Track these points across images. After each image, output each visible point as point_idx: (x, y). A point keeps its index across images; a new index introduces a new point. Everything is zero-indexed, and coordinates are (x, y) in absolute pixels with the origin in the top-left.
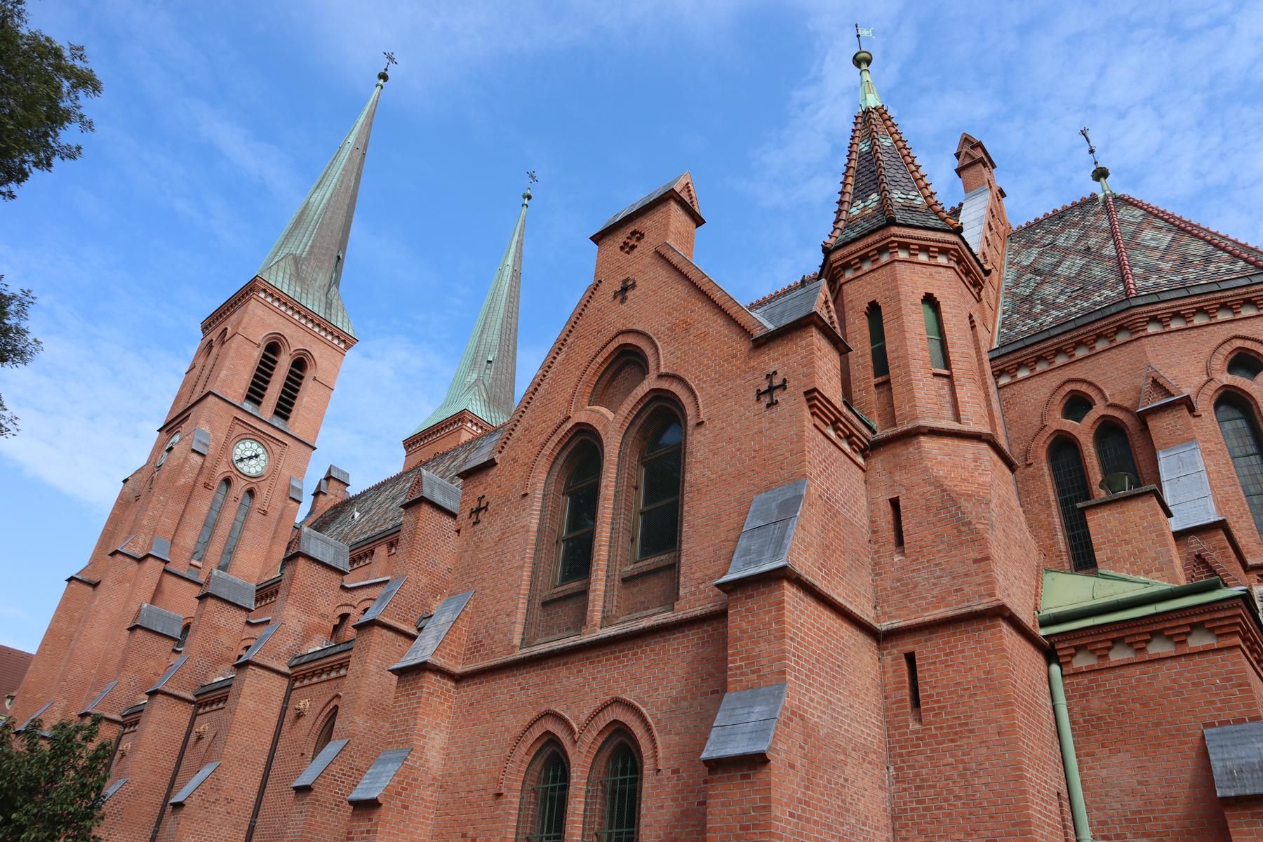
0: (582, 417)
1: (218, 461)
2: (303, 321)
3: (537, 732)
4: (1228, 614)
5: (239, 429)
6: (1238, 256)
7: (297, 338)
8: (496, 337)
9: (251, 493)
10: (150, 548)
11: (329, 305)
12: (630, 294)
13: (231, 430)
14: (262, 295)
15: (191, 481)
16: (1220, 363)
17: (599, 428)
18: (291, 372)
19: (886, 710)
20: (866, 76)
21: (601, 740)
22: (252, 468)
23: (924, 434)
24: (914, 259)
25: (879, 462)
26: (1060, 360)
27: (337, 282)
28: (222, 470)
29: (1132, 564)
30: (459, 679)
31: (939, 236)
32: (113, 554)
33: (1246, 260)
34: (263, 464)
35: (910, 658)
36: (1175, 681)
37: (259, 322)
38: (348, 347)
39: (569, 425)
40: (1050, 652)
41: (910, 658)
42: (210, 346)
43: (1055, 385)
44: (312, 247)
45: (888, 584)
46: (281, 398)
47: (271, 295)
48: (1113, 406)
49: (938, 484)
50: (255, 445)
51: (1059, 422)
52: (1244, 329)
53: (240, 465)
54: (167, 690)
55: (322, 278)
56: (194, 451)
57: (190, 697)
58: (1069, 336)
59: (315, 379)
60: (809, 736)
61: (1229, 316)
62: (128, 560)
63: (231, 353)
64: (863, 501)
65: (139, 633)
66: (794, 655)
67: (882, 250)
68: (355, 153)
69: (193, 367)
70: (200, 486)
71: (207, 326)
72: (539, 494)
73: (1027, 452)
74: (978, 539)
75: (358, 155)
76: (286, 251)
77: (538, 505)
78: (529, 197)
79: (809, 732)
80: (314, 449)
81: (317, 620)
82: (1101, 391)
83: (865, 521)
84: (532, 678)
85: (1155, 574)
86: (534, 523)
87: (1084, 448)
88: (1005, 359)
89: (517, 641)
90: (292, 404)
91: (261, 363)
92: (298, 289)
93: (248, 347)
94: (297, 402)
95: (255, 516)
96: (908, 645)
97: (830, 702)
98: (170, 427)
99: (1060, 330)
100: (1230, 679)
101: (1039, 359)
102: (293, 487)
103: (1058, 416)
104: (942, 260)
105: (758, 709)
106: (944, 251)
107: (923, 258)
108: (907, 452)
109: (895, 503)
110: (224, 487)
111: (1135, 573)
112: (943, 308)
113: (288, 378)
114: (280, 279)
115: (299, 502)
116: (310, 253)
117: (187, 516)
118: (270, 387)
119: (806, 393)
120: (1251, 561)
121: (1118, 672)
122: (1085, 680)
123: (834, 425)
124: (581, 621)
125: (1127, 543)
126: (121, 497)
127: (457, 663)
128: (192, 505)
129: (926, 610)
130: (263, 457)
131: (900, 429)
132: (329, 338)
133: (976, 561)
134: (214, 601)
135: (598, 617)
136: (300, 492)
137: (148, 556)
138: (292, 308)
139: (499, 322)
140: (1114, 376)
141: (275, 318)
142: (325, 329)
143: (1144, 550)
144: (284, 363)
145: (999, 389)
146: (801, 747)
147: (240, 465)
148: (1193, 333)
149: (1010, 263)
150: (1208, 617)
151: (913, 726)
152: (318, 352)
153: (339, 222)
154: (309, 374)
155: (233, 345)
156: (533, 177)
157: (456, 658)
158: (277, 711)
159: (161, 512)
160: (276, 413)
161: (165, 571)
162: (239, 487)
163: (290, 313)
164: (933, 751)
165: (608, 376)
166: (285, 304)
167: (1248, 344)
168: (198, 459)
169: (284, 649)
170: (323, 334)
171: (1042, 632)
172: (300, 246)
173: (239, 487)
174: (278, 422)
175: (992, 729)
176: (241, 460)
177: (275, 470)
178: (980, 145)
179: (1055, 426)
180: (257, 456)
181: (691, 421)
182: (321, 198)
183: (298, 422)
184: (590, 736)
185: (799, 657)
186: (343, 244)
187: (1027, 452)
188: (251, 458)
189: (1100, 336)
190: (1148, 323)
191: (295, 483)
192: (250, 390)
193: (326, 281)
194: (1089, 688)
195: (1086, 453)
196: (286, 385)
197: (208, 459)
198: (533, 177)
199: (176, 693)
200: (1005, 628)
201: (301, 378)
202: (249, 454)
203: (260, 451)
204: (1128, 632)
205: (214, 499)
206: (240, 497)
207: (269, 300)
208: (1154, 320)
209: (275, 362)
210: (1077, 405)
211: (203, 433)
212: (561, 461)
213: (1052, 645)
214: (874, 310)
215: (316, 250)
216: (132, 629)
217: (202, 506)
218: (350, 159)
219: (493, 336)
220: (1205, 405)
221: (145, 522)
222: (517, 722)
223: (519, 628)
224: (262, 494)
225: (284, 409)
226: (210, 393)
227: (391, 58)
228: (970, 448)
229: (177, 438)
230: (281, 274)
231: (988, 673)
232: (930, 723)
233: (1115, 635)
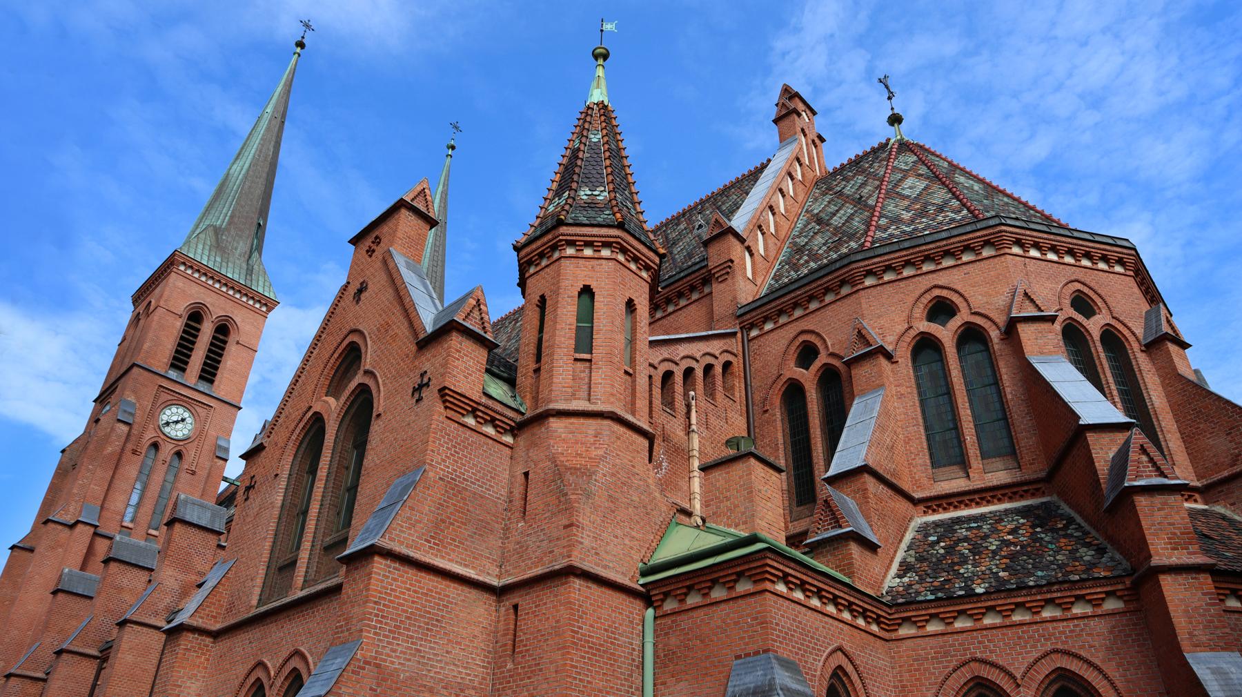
0: (317, 407)
1: (145, 428)
2: (224, 289)
3: (252, 679)
4: (758, 564)
5: (165, 397)
6: (964, 205)
7: (218, 306)
9: (179, 455)
10: (80, 515)
11: (250, 271)
12: (363, 296)
13: (156, 397)
14: (182, 268)
15: (118, 449)
16: (920, 311)
17: (326, 418)
18: (214, 337)
19: (496, 653)
20: (600, 72)
21: (287, 684)
22: (179, 432)
23: (553, 416)
24: (580, 254)
25: (522, 440)
26: (798, 313)
27: (259, 248)
28: (149, 436)
29: (728, 518)
30: (216, 635)
31: (604, 231)
32: (46, 523)
33: (968, 209)
34: (189, 427)
35: (516, 607)
36: (723, 621)
37: (180, 293)
38: (270, 310)
39: (310, 414)
40: (646, 597)
41: (516, 607)
42: (136, 319)
43: (792, 336)
44: (232, 217)
45: (511, 546)
46: (205, 364)
47: (191, 267)
48: (832, 355)
49: (553, 460)
50: (181, 410)
51: (794, 371)
52: (942, 279)
53: (167, 430)
54: (72, 648)
55: (242, 246)
56: (119, 421)
57: (96, 653)
58: (803, 290)
59: (238, 343)
60: (385, 680)
61: (932, 267)
62: (60, 527)
63: (154, 325)
64: (506, 475)
65: (60, 596)
66: (377, 615)
67: (554, 248)
68: (274, 122)
69: (124, 339)
70: (128, 453)
71: (138, 298)
72: (285, 475)
73: (766, 399)
74: (569, 509)
75: (276, 123)
76: (207, 222)
77: (283, 484)
78: (453, 148)
79: (383, 675)
80: (240, 408)
81: (194, 577)
82: (825, 341)
83: (504, 492)
84: (255, 633)
85: (742, 527)
86: (279, 499)
87: (808, 394)
88: (754, 314)
89: (254, 602)
90: (217, 369)
91: (184, 331)
92: (218, 259)
93: (170, 318)
94: (221, 366)
95: (184, 476)
96: (515, 598)
97: (420, 651)
98: (102, 399)
99: (796, 285)
100: (756, 619)
101: (781, 312)
102: (220, 447)
103: (792, 365)
104: (606, 253)
105: (339, 660)
106: (606, 245)
107: (588, 252)
108: (540, 431)
109: (526, 474)
110: (153, 451)
111: (729, 526)
112: (596, 297)
113: (212, 344)
114: (199, 251)
115: (226, 460)
116: (230, 223)
117: (118, 483)
119: (440, 391)
120: (917, 495)
121: (690, 614)
122: (668, 621)
123: (474, 412)
124: (289, 587)
125: (728, 499)
126: (59, 468)
127: (217, 622)
128: (121, 471)
129: (530, 568)
130: (189, 420)
131: (540, 410)
132: (251, 302)
133: (566, 527)
134: (116, 564)
135: (299, 580)
136: (227, 450)
137: (78, 522)
138: (212, 278)
140: (832, 327)
142: (246, 295)
143: (736, 506)
144: (207, 331)
145: (749, 341)
146: (371, 689)
147: (167, 430)
148: (902, 284)
149: (807, 211)
150: (747, 567)
151: (510, 666)
152: (240, 317)
153: (259, 191)
154: (232, 339)
155: (156, 318)
156: (456, 128)
157: (215, 617)
158: (155, 662)
159: (90, 481)
160: (201, 377)
161: (95, 534)
162: (167, 450)
163: (210, 282)
164: (517, 686)
165: (342, 368)
166: (205, 274)
167: (944, 293)
168: (125, 428)
169: (161, 606)
170: (244, 299)
171: (642, 581)
172: (220, 218)
173: (167, 450)
174: (203, 386)
175: (552, 668)
176: (168, 424)
177: (201, 432)
178: (797, 95)
179: (788, 374)
180: (183, 420)
181: (374, 415)
182: (240, 169)
183: (223, 385)
184: (278, 682)
185: (383, 617)
186: (264, 212)
187: (766, 399)
188: (178, 422)
189: (827, 290)
190: (865, 276)
191: (222, 443)
192: (174, 358)
193: (247, 249)
194: (671, 628)
195: (809, 399)
196: (210, 351)
197: (135, 426)
198: (456, 128)
199: (81, 650)
200: (577, 583)
201: (225, 342)
202: (175, 418)
203: (186, 415)
204: (697, 580)
205: (143, 462)
206: (168, 459)
207: (189, 272)
208: (870, 273)
209: (198, 330)
210: (807, 354)
211: (129, 403)
212: (304, 446)
213: (648, 591)
214: (543, 299)
215: (236, 220)
216: (55, 593)
217: (131, 469)
218: (268, 129)
220: (904, 355)
221: (75, 491)
222: (242, 670)
223: (257, 591)
224: (190, 455)
225: (209, 373)
226: (134, 365)
227: (307, 26)
228: (592, 425)
229: (108, 408)
230: (200, 246)
231: (558, 621)
232: (519, 663)
233: (688, 583)
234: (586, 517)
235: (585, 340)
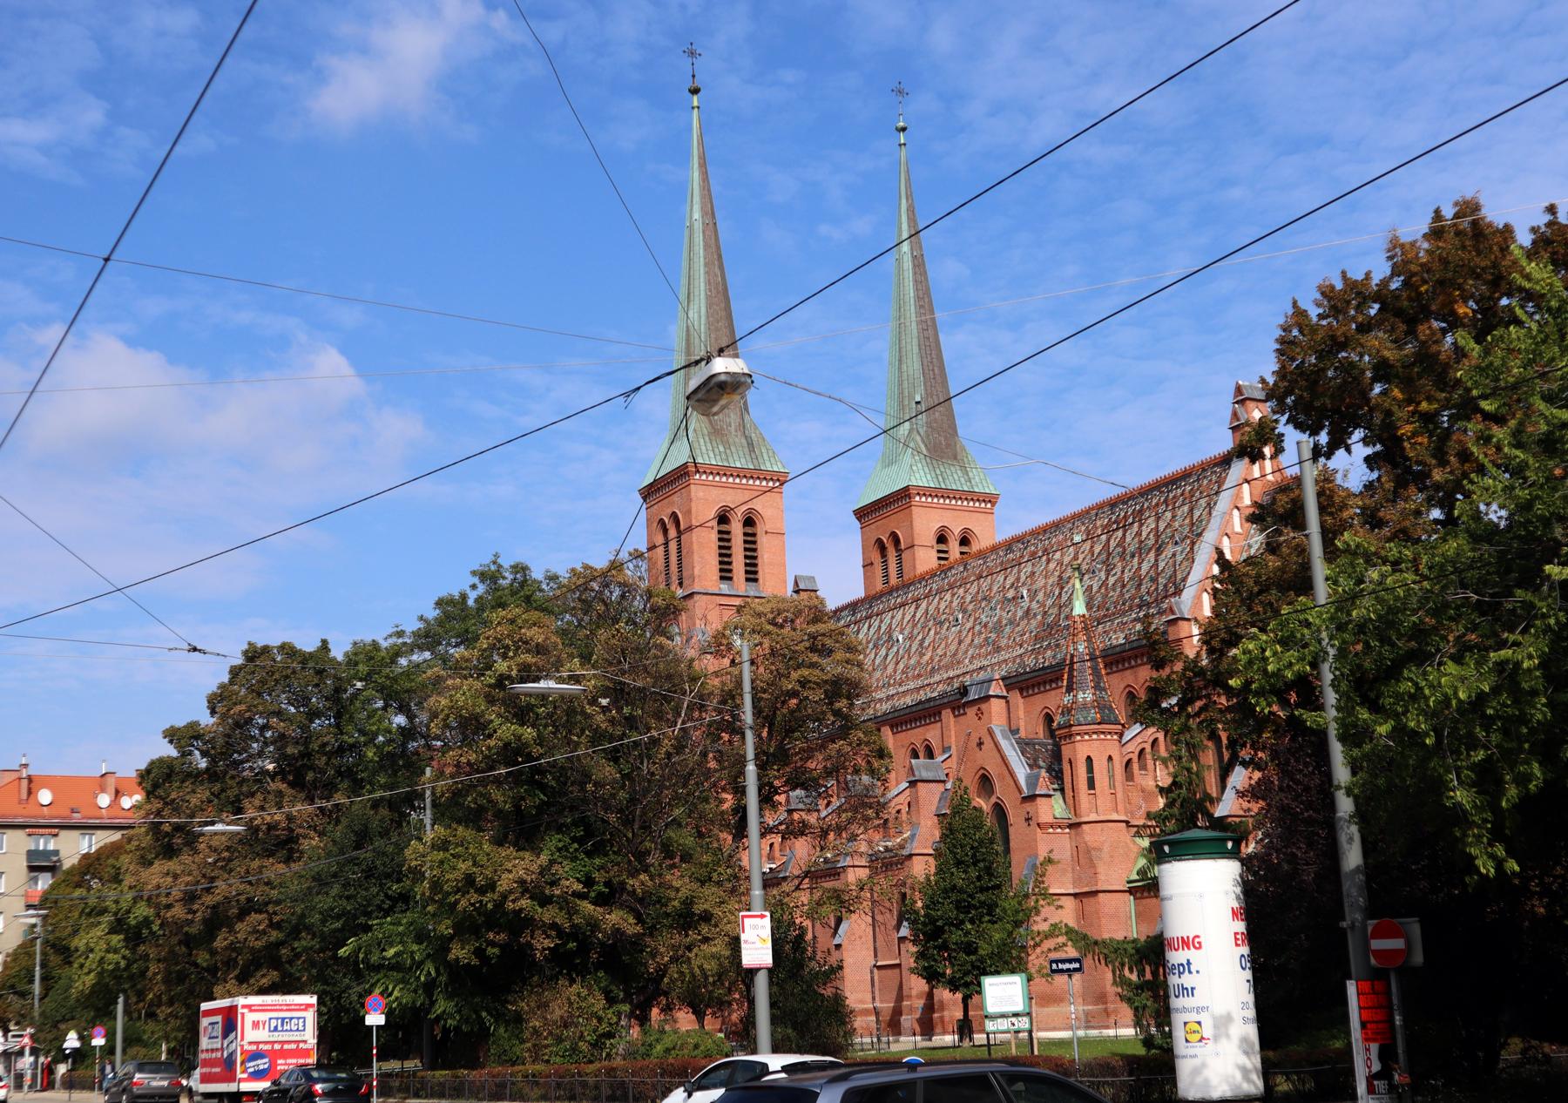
8: (917, 365)
74: (1093, 866)
94: (759, 561)
118: (734, 559)
139: (915, 342)
141: (715, 492)
144: (737, 528)
154: (760, 529)
219: (914, 365)
234: (1101, 869)
235: (1091, 784)
